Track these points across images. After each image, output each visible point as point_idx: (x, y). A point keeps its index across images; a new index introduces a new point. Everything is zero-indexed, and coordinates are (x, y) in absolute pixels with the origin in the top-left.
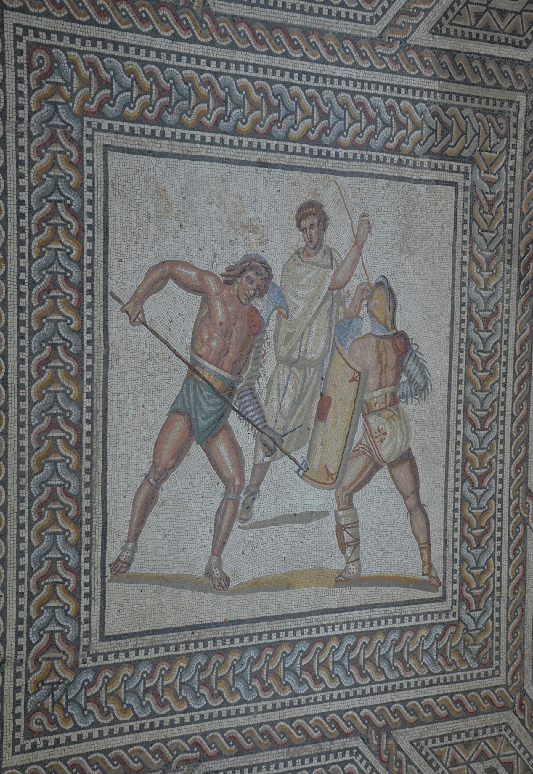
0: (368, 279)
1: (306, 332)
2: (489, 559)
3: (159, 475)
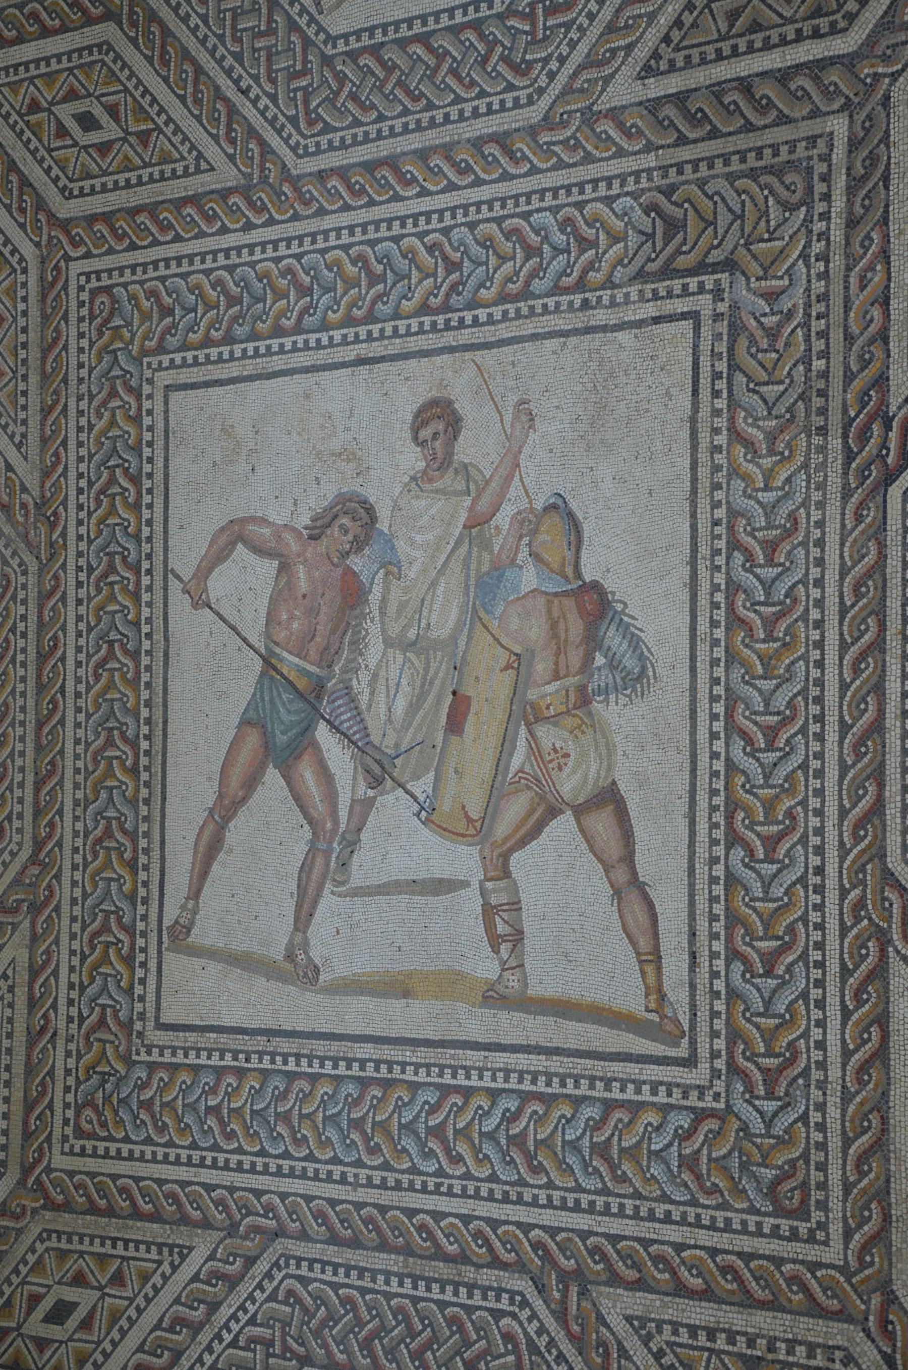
0: (530, 502)
1: (428, 597)
2: (795, 1001)
3: (226, 809)
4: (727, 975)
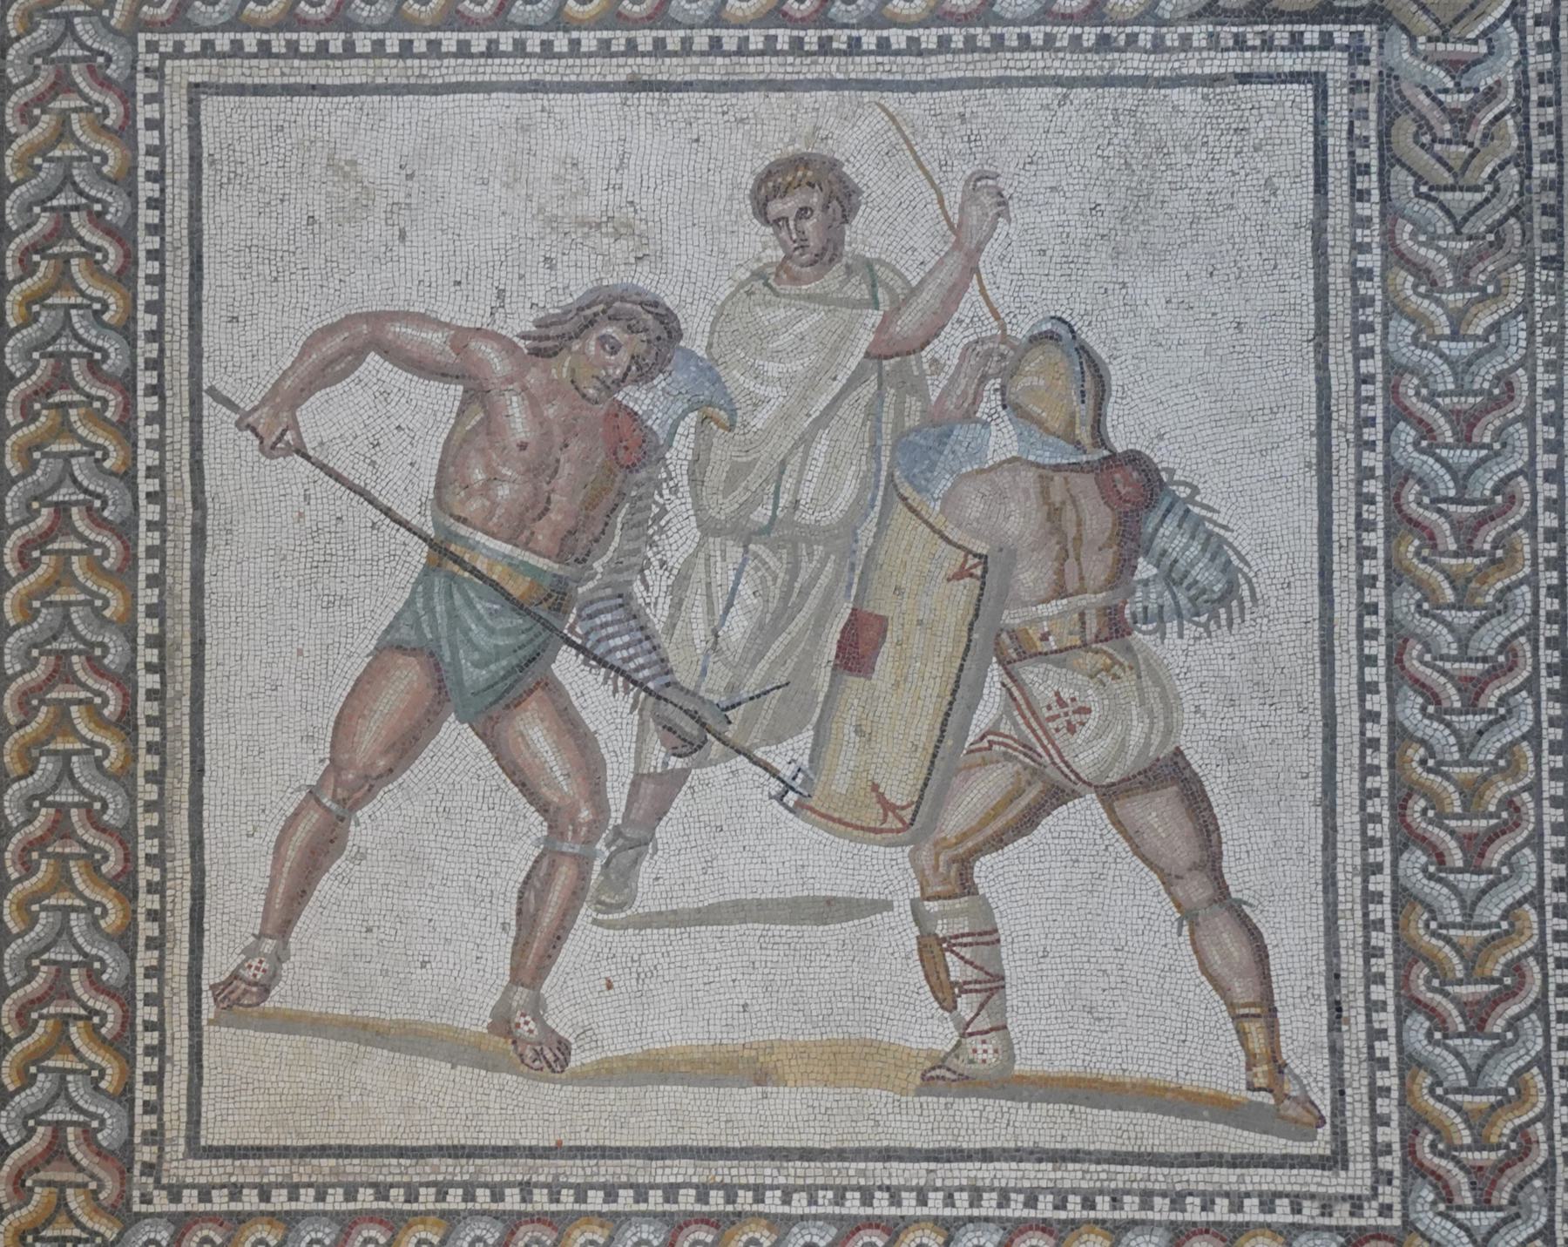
0: (1003, 327)
1: (796, 460)
2: (1528, 1067)
4: (1399, 1035)
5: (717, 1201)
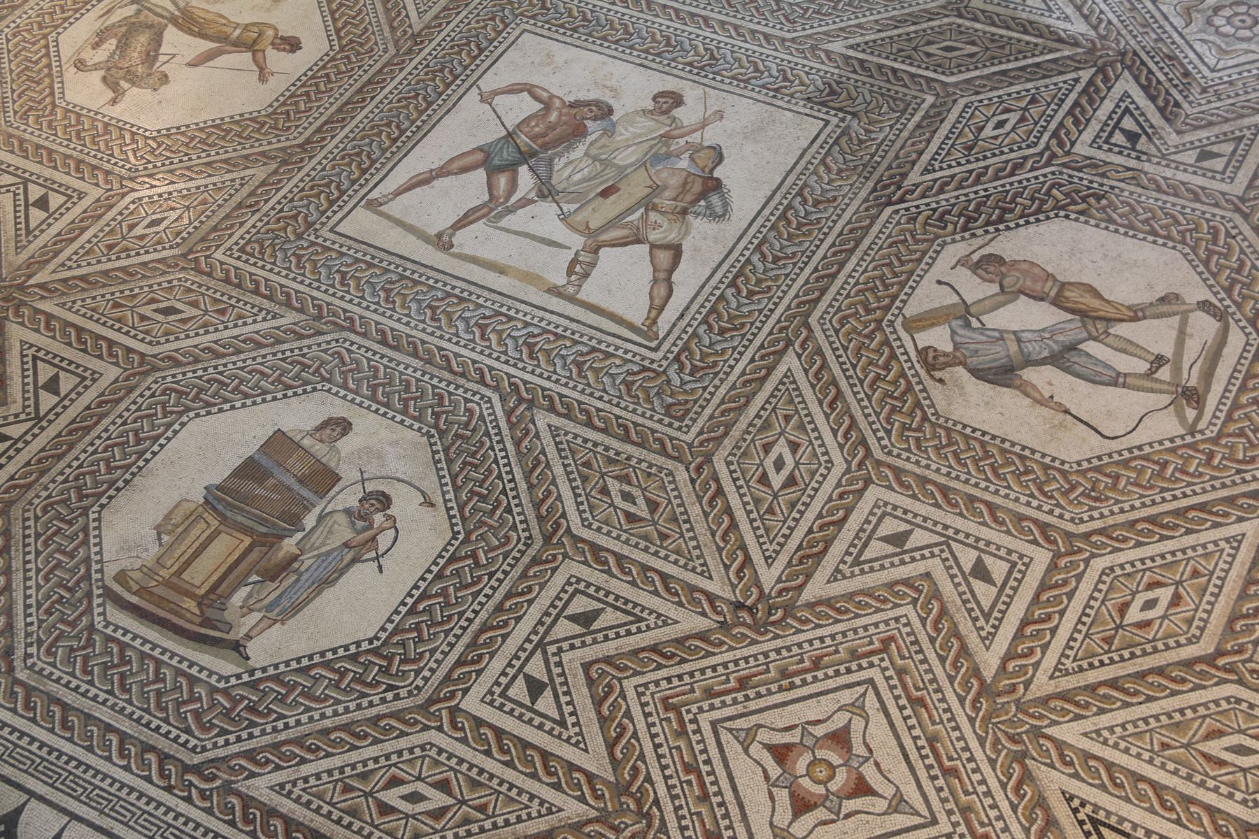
3: (443, 172)
5: (465, 294)
